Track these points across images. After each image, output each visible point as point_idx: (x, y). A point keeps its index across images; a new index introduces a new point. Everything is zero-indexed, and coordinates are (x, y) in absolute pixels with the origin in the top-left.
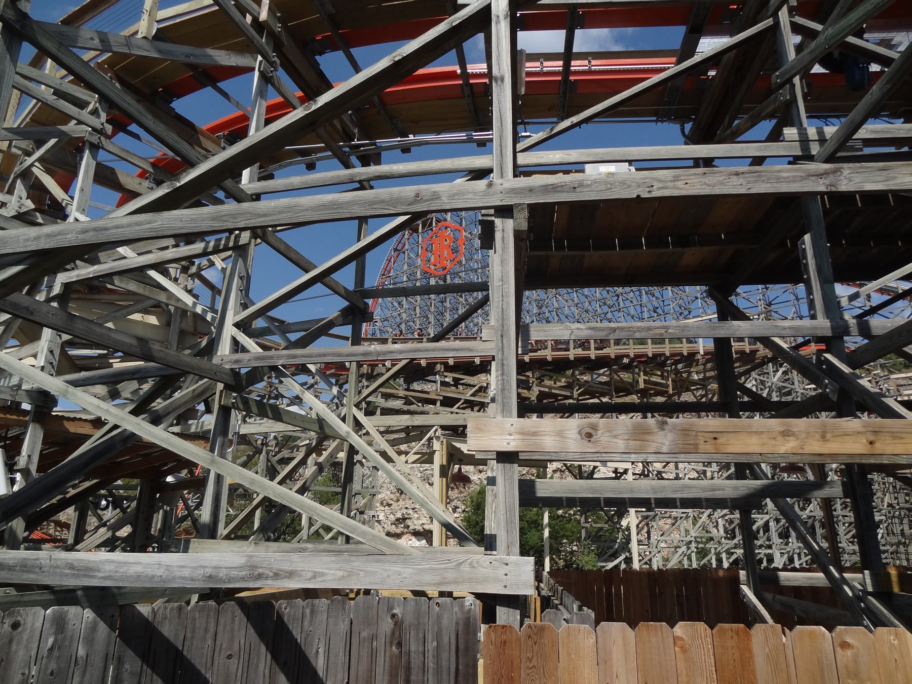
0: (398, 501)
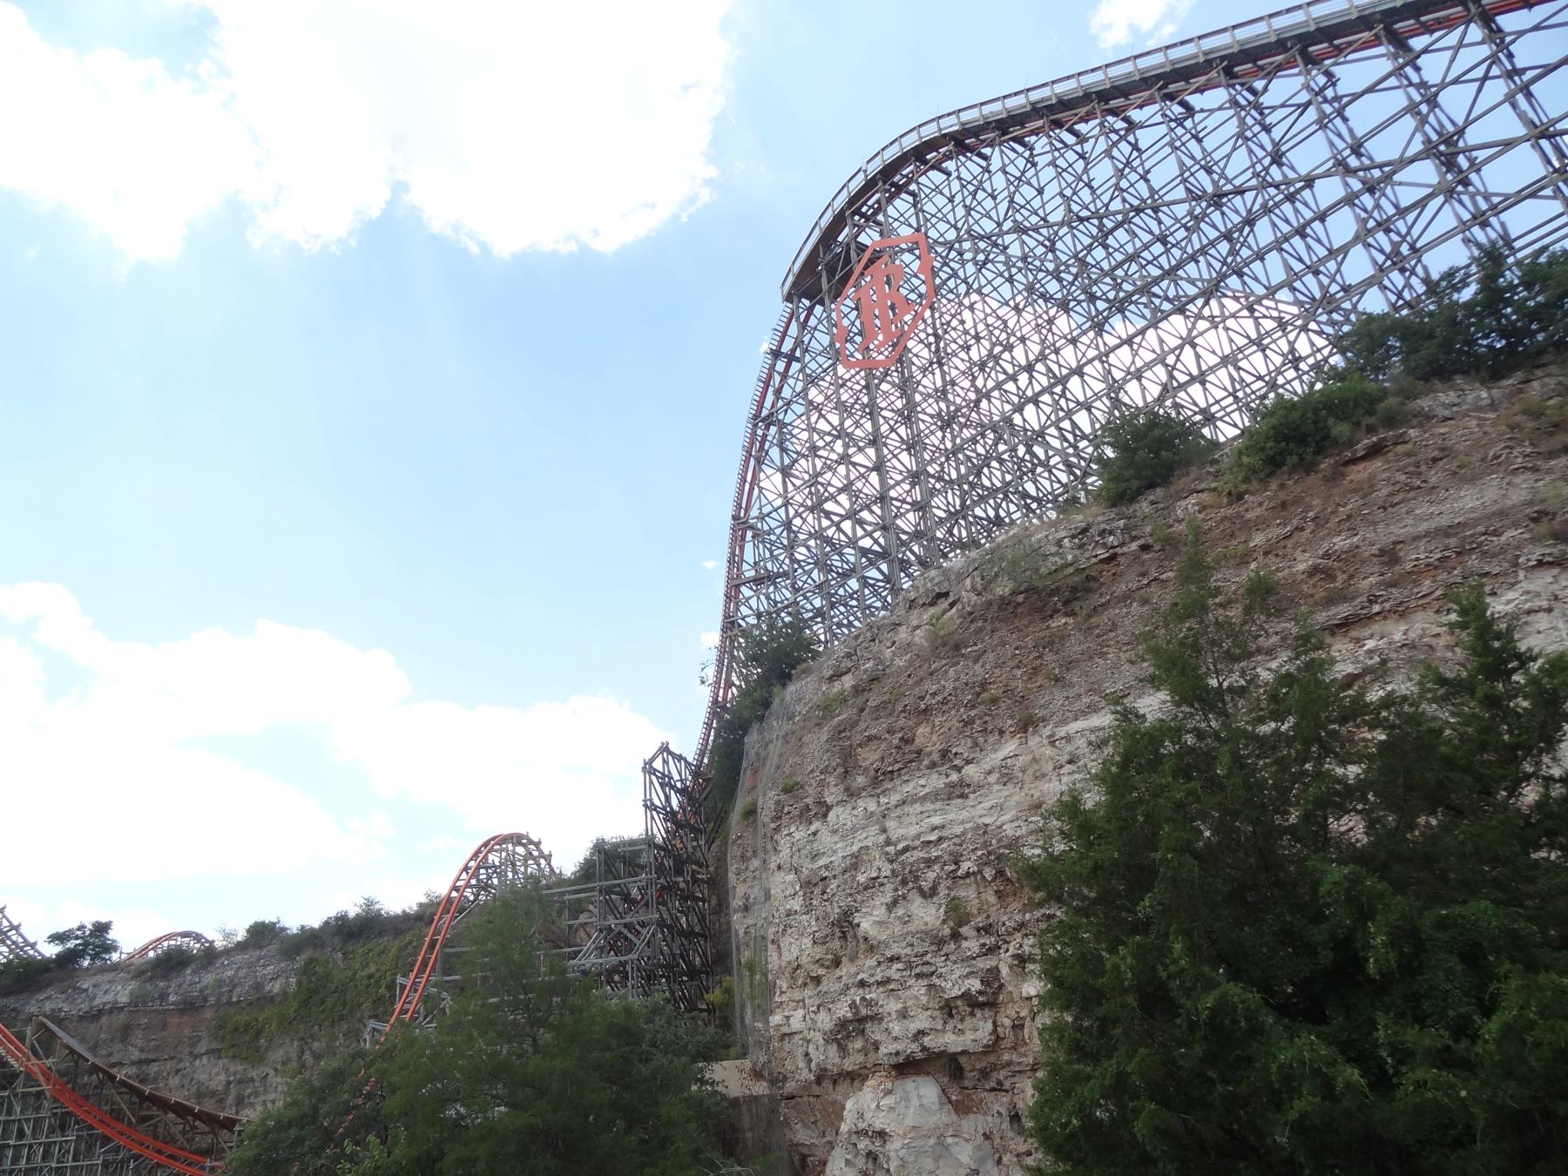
0: (837, 963)
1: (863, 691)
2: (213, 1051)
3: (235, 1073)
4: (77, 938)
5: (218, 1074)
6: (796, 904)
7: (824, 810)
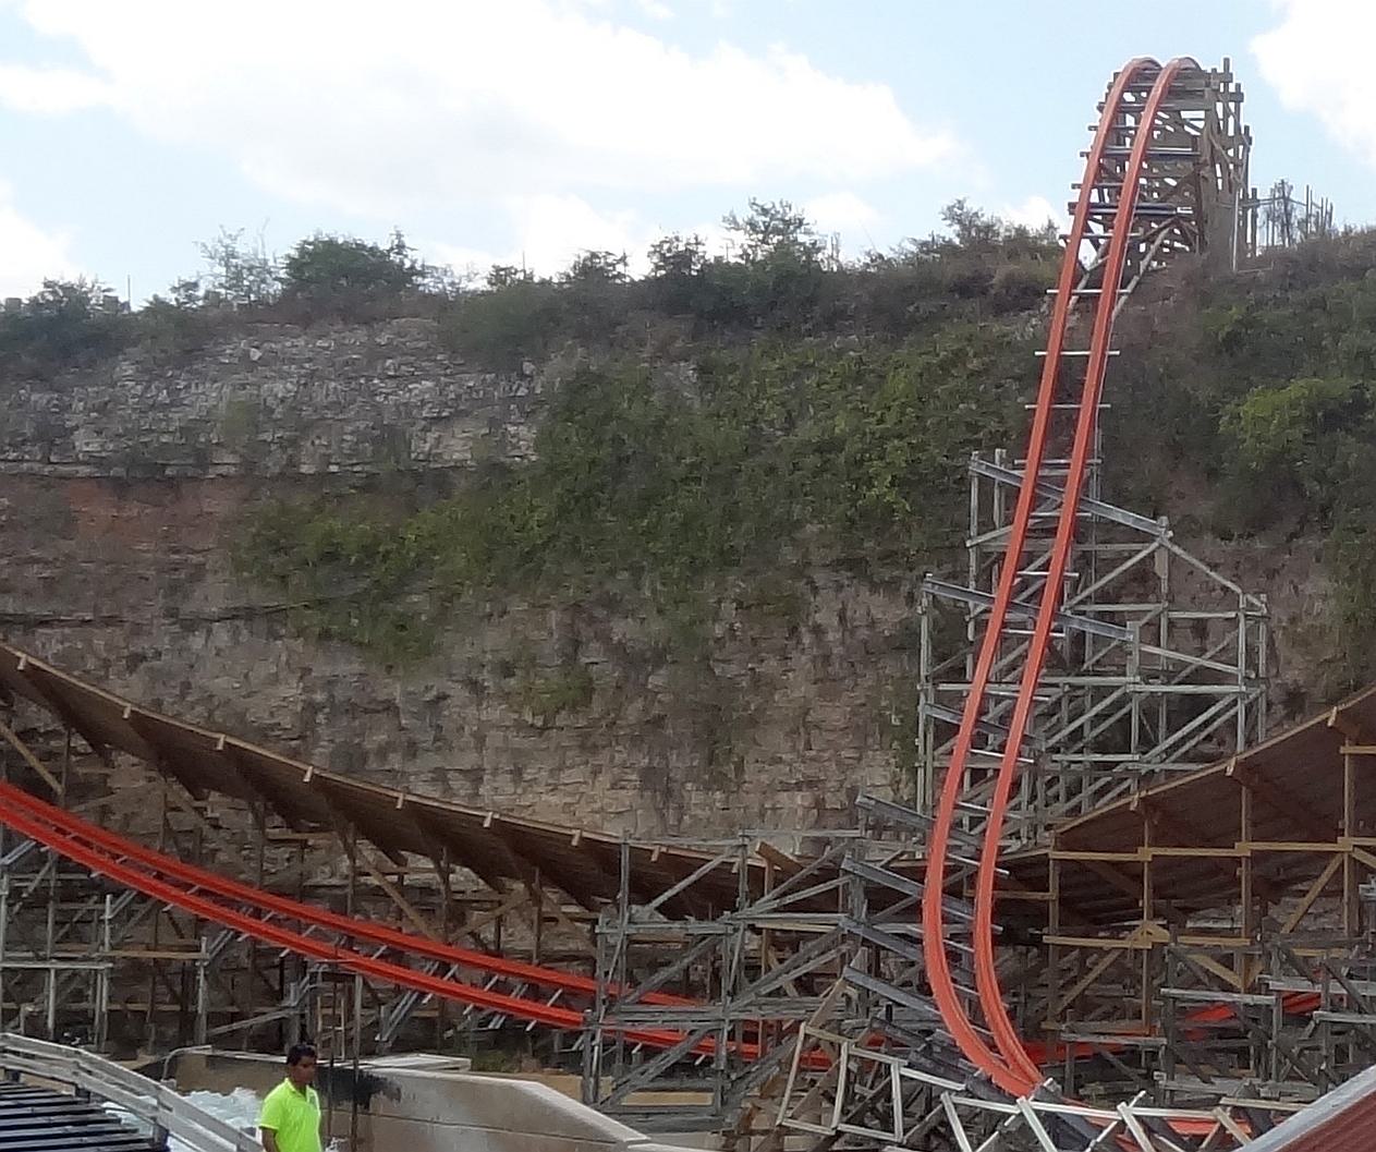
2: (249, 614)
3: (330, 683)
5: (274, 680)
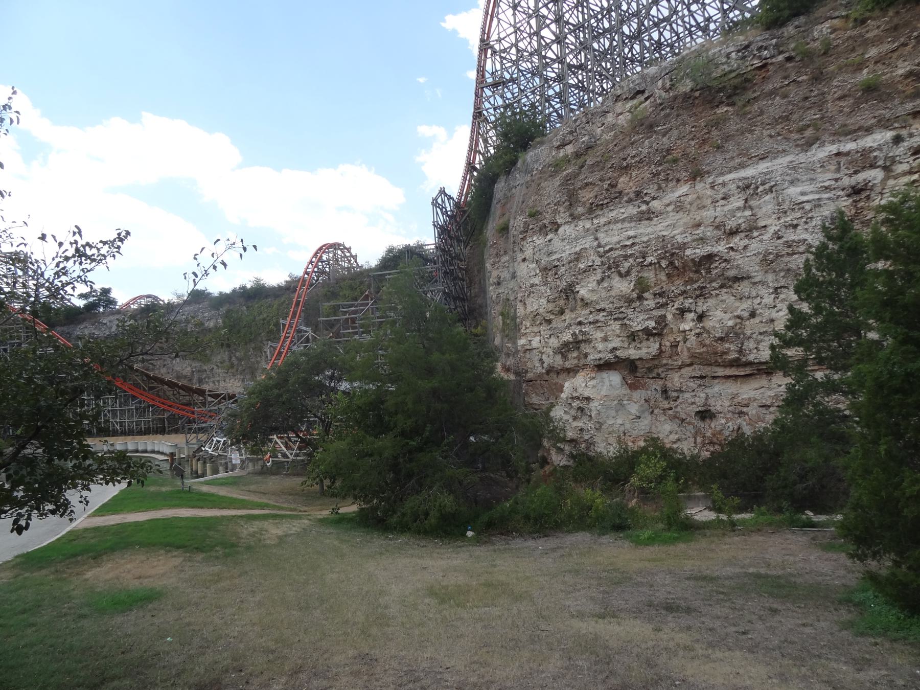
0: (562, 312)
1: (581, 155)
3: (195, 367)
4: (94, 296)
5: (186, 367)
6: (537, 281)
7: (556, 227)
